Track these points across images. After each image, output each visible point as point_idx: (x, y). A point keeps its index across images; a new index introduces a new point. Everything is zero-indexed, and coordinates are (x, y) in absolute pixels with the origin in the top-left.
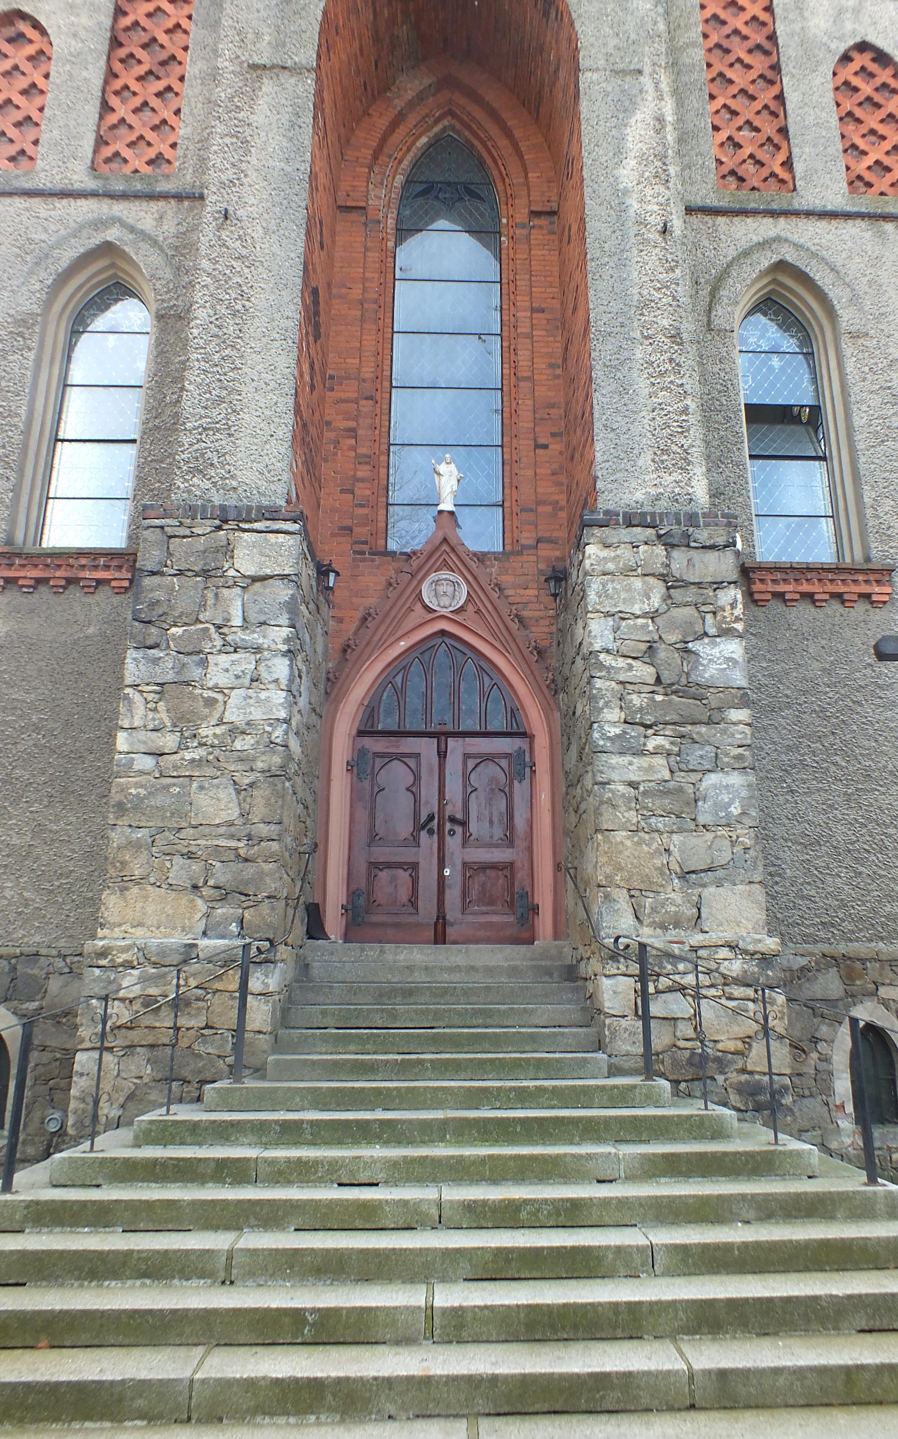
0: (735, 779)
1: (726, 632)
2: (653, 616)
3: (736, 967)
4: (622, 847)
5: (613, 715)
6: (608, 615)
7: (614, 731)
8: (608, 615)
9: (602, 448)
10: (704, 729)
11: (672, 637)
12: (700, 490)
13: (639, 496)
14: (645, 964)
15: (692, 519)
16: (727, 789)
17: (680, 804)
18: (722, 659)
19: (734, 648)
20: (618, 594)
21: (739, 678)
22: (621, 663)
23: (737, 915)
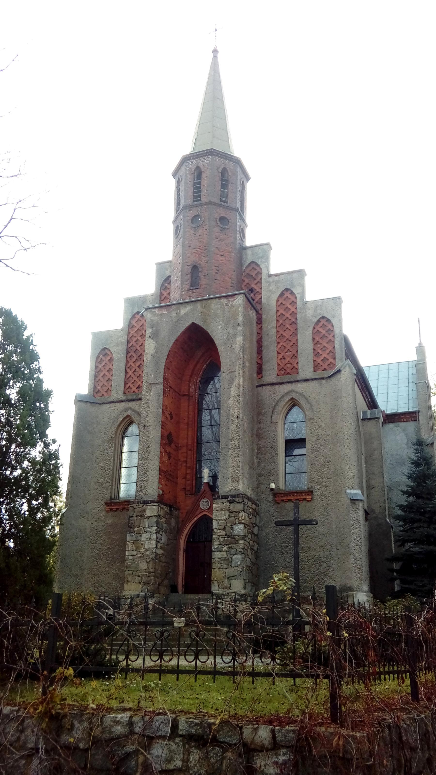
0: (239, 556)
2: (226, 520)
10: (234, 545)
11: (229, 525)
13: (228, 489)
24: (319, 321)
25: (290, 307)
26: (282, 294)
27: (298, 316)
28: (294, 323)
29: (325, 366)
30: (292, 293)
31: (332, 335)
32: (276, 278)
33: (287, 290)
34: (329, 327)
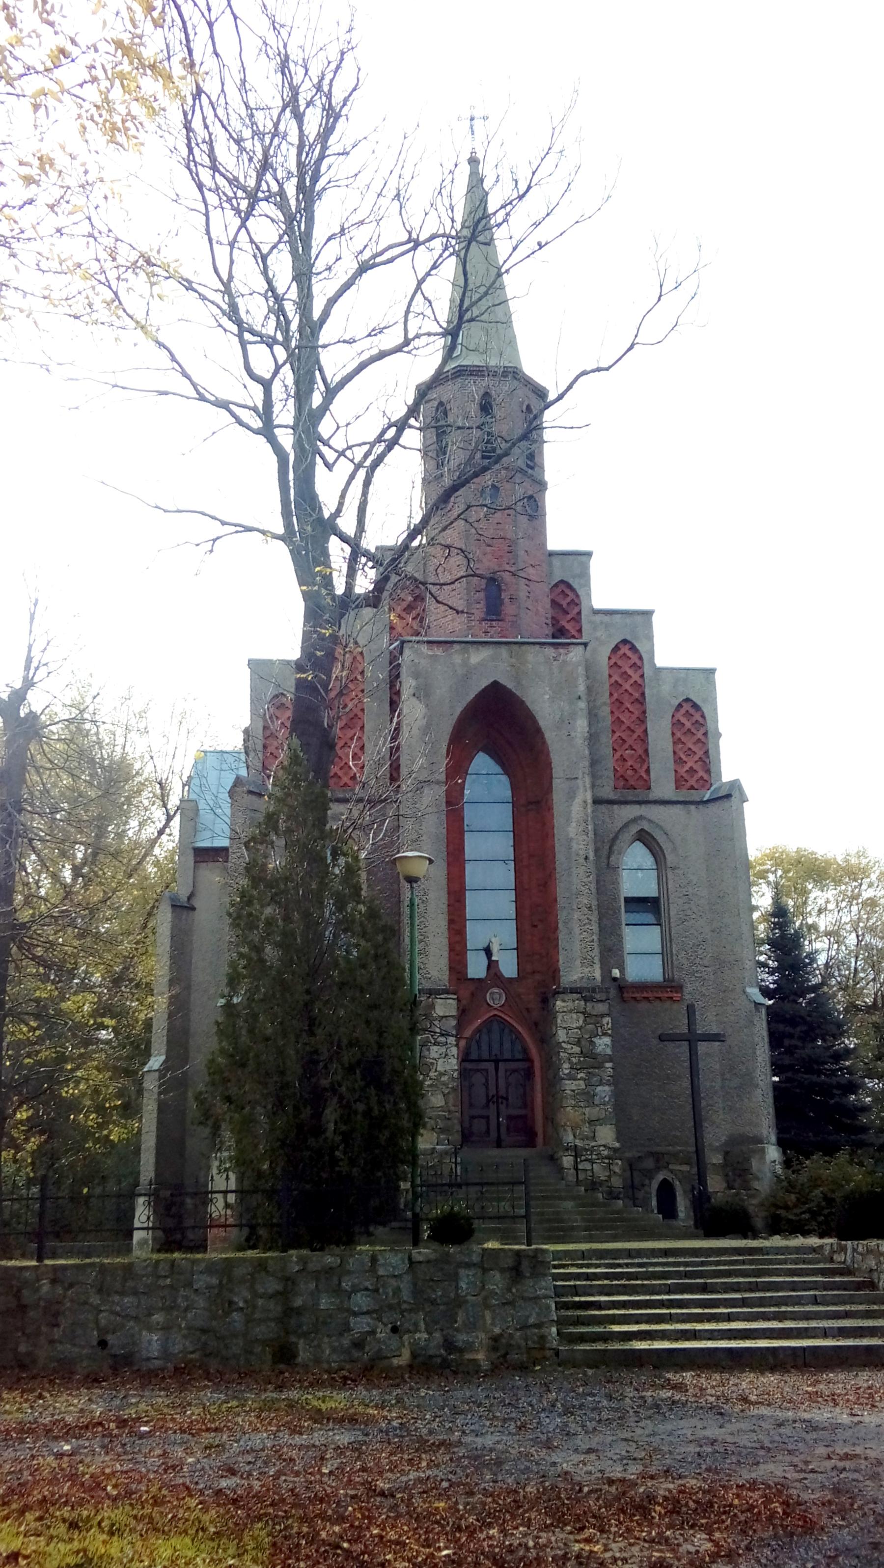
1: (605, 1034)
2: (580, 1028)
3: (606, 1153)
4: (570, 1113)
5: (566, 1068)
7: (567, 1071)
12: (598, 974)
13: (575, 977)
14: (577, 1152)
15: (594, 990)
16: (604, 1091)
17: (588, 1097)
18: (603, 1044)
19: (607, 1040)
20: (567, 1020)
21: (609, 1051)
22: (569, 1046)
23: (606, 1135)
24: (680, 706)
26: (616, 649)
27: (647, 692)
28: (641, 701)
30: (633, 648)
31: (702, 731)
33: (625, 642)
34: (697, 717)
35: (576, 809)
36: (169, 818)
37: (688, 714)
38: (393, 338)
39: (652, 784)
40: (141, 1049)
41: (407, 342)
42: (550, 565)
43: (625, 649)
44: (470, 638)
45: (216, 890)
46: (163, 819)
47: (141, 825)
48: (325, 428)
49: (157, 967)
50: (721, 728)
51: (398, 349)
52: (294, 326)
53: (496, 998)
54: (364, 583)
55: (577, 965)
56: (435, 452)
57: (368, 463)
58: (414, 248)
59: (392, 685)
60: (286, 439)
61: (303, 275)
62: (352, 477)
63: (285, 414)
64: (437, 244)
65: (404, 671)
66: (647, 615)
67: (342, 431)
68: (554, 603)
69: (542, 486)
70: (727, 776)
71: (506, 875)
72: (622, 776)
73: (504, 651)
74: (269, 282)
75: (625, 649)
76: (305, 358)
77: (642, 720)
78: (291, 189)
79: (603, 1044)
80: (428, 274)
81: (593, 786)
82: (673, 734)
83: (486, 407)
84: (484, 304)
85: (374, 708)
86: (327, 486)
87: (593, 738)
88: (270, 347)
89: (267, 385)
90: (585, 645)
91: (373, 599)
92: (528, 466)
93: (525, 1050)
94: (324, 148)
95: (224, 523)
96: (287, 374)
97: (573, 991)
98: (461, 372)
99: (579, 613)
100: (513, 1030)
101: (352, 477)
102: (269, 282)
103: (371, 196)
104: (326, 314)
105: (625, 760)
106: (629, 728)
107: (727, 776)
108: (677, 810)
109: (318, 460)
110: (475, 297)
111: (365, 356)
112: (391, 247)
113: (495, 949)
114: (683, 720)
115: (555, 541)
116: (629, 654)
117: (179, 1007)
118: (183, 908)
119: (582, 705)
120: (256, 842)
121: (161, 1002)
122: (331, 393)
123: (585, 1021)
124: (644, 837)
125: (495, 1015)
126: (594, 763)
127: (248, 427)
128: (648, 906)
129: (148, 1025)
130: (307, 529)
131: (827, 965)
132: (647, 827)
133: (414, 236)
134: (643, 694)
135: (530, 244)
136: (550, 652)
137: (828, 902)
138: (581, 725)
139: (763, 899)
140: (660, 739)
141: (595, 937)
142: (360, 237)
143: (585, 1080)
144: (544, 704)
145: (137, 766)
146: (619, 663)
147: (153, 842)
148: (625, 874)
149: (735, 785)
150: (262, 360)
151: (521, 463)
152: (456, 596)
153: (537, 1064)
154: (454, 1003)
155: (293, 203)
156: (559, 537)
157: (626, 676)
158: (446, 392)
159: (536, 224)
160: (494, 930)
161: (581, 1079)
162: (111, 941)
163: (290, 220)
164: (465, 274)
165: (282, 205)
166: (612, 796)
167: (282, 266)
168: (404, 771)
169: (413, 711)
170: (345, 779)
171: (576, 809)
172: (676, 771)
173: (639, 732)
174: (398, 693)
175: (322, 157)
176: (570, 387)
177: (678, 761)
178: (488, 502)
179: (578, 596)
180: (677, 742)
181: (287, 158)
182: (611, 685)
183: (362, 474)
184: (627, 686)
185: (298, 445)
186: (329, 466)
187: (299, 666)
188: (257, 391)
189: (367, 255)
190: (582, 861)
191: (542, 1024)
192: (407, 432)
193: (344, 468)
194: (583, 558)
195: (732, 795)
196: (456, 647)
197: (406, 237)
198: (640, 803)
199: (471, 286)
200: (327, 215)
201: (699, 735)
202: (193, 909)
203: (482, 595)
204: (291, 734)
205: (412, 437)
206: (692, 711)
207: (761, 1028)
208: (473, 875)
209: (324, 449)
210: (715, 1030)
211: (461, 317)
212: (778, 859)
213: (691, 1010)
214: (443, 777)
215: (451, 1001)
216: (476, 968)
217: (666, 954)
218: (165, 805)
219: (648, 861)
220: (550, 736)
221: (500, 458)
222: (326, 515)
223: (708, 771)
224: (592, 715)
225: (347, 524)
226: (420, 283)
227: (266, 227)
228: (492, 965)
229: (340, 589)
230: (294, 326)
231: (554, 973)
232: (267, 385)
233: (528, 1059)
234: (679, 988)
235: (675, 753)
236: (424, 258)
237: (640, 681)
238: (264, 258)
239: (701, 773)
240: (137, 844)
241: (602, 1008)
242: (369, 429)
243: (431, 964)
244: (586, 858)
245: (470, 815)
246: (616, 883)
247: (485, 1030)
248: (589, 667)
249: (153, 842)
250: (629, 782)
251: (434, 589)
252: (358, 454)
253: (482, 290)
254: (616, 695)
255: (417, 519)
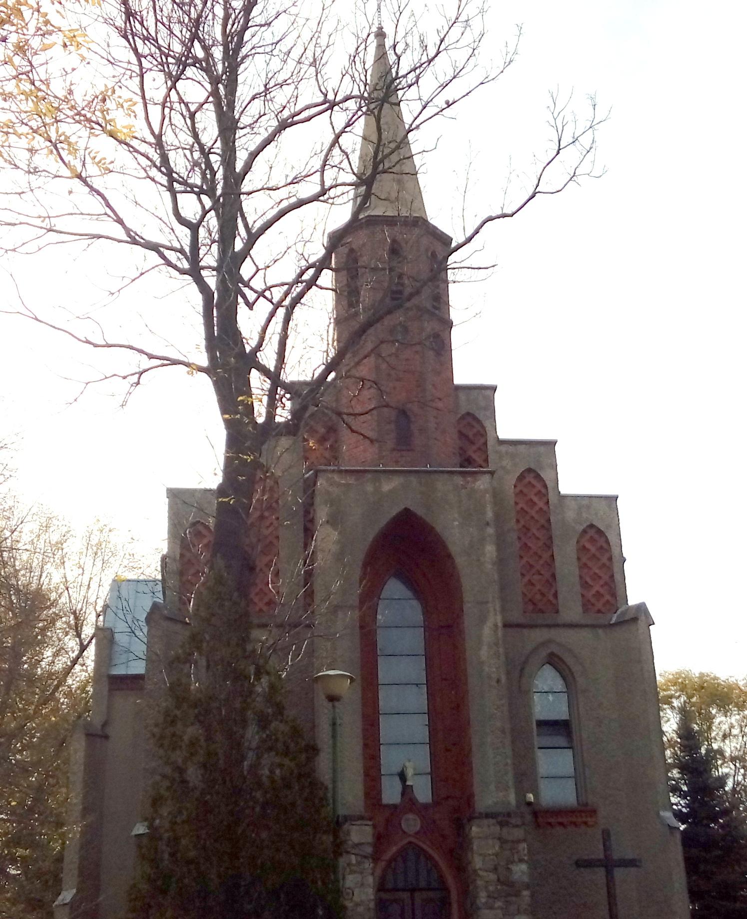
1: (521, 861)
2: (496, 855)
5: (482, 898)
6: (481, 855)
7: (483, 900)
8: (481, 855)
9: (476, 780)
12: (512, 798)
13: (490, 802)
15: (509, 815)
18: (520, 870)
19: (524, 867)
20: (483, 845)
21: (526, 879)
22: (485, 874)
24: (584, 532)
25: (535, 499)
26: (521, 478)
28: (547, 526)
29: (599, 605)
30: (538, 477)
31: (607, 555)
32: (511, 449)
33: (530, 470)
34: (601, 542)
35: (487, 630)
36: (83, 648)
37: (592, 540)
38: (309, 188)
39: (560, 609)
40: (55, 883)
41: (324, 192)
42: (457, 397)
43: (530, 478)
44: (381, 468)
45: (131, 723)
46: (77, 649)
47: (56, 655)
48: (246, 270)
49: (71, 797)
50: (626, 553)
51: (315, 198)
52: (220, 175)
53: (411, 823)
54: (283, 415)
55: (492, 790)
56: (347, 295)
57: (287, 302)
58: (331, 108)
59: (307, 512)
60: (212, 281)
61: (228, 127)
62: (272, 315)
63: (210, 257)
64: (352, 105)
65: (318, 500)
66: (550, 445)
67: (261, 273)
68: (462, 435)
69: (448, 325)
70: (632, 601)
71: (418, 699)
72: (530, 600)
73: (413, 479)
74: (196, 136)
75: (530, 478)
76: (229, 207)
77: (548, 545)
78: (218, 53)
79: (520, 870)
80: (343, 131)
81: (503, 610)
82: (579, 559)
83: (395, 250)
84: (394, 158)
85: (288, 532)
86: (249, 322)
87: (501, 562)
88: (198, 195)
89: (194, 228)
90: (492, 473)
91: (291, 428)
92: (434, 307)
93: (441, 877)
94: (247, 21)
95: (151, 357)
96: (212, 220)
97: (488, 816)
98: (373, 221)
99: (485, 444)
100: (429, 858)
101: (272, 315)
102: (196, 136)
103: (291, 64)
104: (248, 167)
105: (533, 584)
106: (536, 553)
107: (632, 601)
108: (586, 634)
109: (240, 300)
110: (387, 151)
111: (285, 204)
112: (308, 107)
113: (410, 772)
114: (588, 545)
115: (461, 377)
116: (534, 482)
117: (91, 841)
118: (97, 736)
119: (490, 530)
120: (177, 663)
121: (74, 831)
122: (253, 238)
123: (501, 847)
124: (555, 661)
125: (410, 843)
126: (503, 588)
127: (175, 267)
128: (559, 728)
129: (60, 859)
130: (229, 361)
131: (734, 789)
132: (554, 649)
133: (331, 97)
134: (549, 520)
135: (440, 101)
136: (459, 480)
137: (732, 727)
138: (490, 550)
139: (670, 724)
140: (569, 562)
141: (509, 761)
142: (280, 97)
143: (502, 908)
144: (453, 530)
145: (53, 596)
146: (525, 491)
147: (68, 671)
148: (536, 697)
149: (642, 609)
150: (190, 206)
151: (428, 305)
152: (367, 425)
153: (454, 896)
154: (369, 829)
155: (220, 67)
156: (465, 371)
157: (532, 503)
158: (358, 240)
159: (444, 86)
160: (408, 756)
161: (499, 908)
162: (25, 769)
163: (215, 81)
164: (379, 129)
165: (208, 70)
166: (522, 620)
167: (208, 125)
168: (319, 596)
169: (326, 538)
170: (261, 605)
171: (487, 630)
172: (583, 596)
173: (546, 556)
174: (312, 521)
175: (245, 28)
176: (477, 232)
177: (585, 585)
178: (400, 337)
179: (483, 427)
180: (583, 566)
181: (214, 30)
182: (518, 512)
183: (281, 312)
184: (533, 513)
185: (222, 283)
186: (250, 306)
187: (221, 491)
188: (184, 234)
189: (286, 114)
190: (494, 683)
191: (458, 853)
192: (325, 271)
193: (264, 307)
194: (488, 392)
195: (640, 618)
196: (369, 476)
197: (321, 99)
198: (549, 626)
199: (384, 141)
200: (250, 78)
201: (604, 560)
202: (106, 737)
203: (393, 426)
204: (214, 555)
205: (327, 278)
206: (596, 537)
207: (676, 853)
208: (387, 699)
209: (246, 290)
210: (630, 855)
211: (375, 166)
212: (683, 684)
213: (606, 835)
214: (357, 603)
215: (367, 828)
216: (391, 793)
217: (579, 777)
218: (79, 635)
219: (559, 685)
220: (460, 561)
221: (411, 296)
222: (248, 349)
223: (614, 595)
224: (500, 541)
225: (268, 358)
226: (338, 136)
227: (194, 88)
228: (406, 790)
229: (261, 420)
230: (220, 175)
231: (469, 800)
232: (194, 228)
233: (444, 888)
234: (593, 812)
235: (581, 577)
236: (340, 118)
237: (545, 508)
238: (192, 116)
239: (608, 597)
240: (50, 675)
241: (518, 833)
242: (286, 271)
243: (350, 794)
244: (498, 681)
245: (382, 639)
246: (528, 706)
247: (399, 859)
248: (497, 495)
249: (68, 671)
250: (537, 605)
251: (350, 419)
252: (277, 294)
253: (393, 145)
254: (522, 522)
255: (332, 353)
